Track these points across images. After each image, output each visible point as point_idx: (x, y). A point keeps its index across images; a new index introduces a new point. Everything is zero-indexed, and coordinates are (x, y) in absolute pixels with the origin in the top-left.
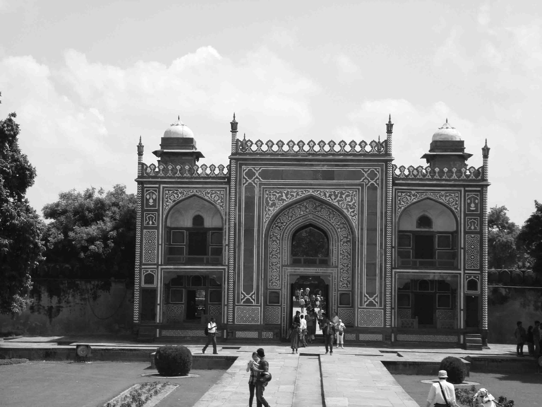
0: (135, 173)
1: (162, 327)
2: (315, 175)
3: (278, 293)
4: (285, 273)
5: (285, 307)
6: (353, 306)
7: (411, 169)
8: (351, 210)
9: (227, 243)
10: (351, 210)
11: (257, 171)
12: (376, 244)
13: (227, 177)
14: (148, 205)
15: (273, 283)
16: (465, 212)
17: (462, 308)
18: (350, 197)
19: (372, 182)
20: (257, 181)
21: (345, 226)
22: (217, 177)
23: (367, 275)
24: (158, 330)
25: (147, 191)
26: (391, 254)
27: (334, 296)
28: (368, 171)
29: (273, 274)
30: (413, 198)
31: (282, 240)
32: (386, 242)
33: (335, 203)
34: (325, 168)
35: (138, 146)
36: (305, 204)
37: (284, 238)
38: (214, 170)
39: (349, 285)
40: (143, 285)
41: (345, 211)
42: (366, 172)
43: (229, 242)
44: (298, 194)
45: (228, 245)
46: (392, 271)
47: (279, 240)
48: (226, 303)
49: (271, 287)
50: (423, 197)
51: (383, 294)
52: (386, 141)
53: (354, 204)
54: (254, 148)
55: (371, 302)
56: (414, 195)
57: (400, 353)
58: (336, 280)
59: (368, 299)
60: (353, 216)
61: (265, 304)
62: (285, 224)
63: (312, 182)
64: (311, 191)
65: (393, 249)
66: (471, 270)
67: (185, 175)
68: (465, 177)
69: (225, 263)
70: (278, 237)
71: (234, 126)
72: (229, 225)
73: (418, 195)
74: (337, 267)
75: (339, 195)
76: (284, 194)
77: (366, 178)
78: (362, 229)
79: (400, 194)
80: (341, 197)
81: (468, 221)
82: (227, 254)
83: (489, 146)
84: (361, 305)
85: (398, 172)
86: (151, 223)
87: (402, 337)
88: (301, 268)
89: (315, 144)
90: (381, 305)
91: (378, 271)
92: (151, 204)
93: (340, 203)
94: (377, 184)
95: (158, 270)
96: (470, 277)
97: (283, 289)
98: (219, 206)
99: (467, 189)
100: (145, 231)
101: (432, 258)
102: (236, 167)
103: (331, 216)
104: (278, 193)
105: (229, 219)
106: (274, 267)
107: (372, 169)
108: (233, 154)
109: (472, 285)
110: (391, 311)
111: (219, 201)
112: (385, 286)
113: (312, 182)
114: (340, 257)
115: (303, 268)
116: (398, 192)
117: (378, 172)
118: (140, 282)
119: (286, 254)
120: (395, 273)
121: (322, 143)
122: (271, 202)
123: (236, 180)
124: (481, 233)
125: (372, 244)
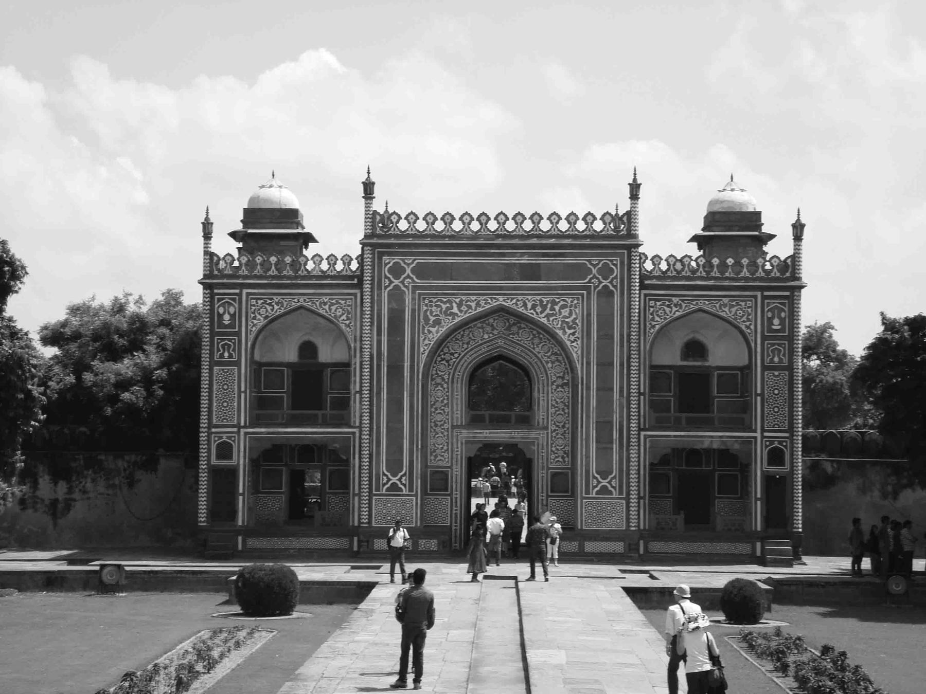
0: (198, 271)
1: (248, 532)
2: (508, 272)
3: (445, 474)
5: (458, 496)
6: (573, 494)
7: (672, 260)
8: (569, 332)
9: (358, 389)
11: (408, 265)
12: (612, 389)
13: (357, 276)
14: (221, 325)
15: (436, 456)
16: (762, 332)
17: (759, 496)
19: (605, 283)
20: (408, 281)
21: (560, 358)
22: (339, 276)
23: (597, 442)
24: (240, 538)
25: (219, 300)
26: (638, 406)
27: (541, 476)
28: (598, 264)
29: (438, 441)
30: (674, 309)
31: (452, 382)
32: (629, 385)
33: (542, 320)
34: (525, 260)
35: (203, 223)
36: (491, 321)
37: (455, 380)
38: (335, 263)
39: (566, 459)
40: (214, 461)
41: (560, 332)
42: (594, 266)
43: (361, 387)
44: (478, 305)
45: (360, 392)
46: (639, 434)
48: (357, 492)
49: (434, 463)
50: (693, 307)
51: (624, 473)
52: (629, 214)
53: (574, 321)
54: (403, 225)
55: (604, 487)
56: (676, 305)
57: (654, 574)
59: (599, 482)
60: (572, 342)
61: (424, 492)
62: (456, 355)
64: (501, 298)
65: (642, 397)
66: (774, 432)
67: (285, 273)
68: (763, 274)
69: (355, 422)
70: (446, 377)
71: (368, 188)
72: (361, 357)
73: (684, 305)
74: (546, 428)
75: (549, 306)
76: (454, 304)
77: (594, 277)
78: (588, 364)
79: (652, 303)
80: (552, 309)
81: (768, 348)
82: (359, 407)
83: (803, 221)
84: (587, 492)
85: (648, 266)
86: (226, 354)
87: (657, 546)
88: (485, 431)
89: (507, 219)
90: (621, 493)
91: (615, 435)
92: (227, 323)
93: (551, 319)
94: (614, 286)
95: (239, 436)
96: (772, 443)
97: (454, 466)
98: (343, 326)
99: (766, 293)
100: (216, 368)
101: (708, 413)
102: (373, 258)
103: (536, 341)
104: (445, 303)
105: (361, 348)
106: (438, 429)
107: (605, 260)
108: (366, 236)
109: (776, 456)
110: (639, 503)
111: (344, 317)
112: (628, 461)
114: (552, 410)
115: (488, 431)
116: (650, 300)
117: (616, 265)
118: (209, 457)
121: (519, 217)
122: (432, 319)
123: (373, 280)
124: (790, 368)
125: (605, 388)
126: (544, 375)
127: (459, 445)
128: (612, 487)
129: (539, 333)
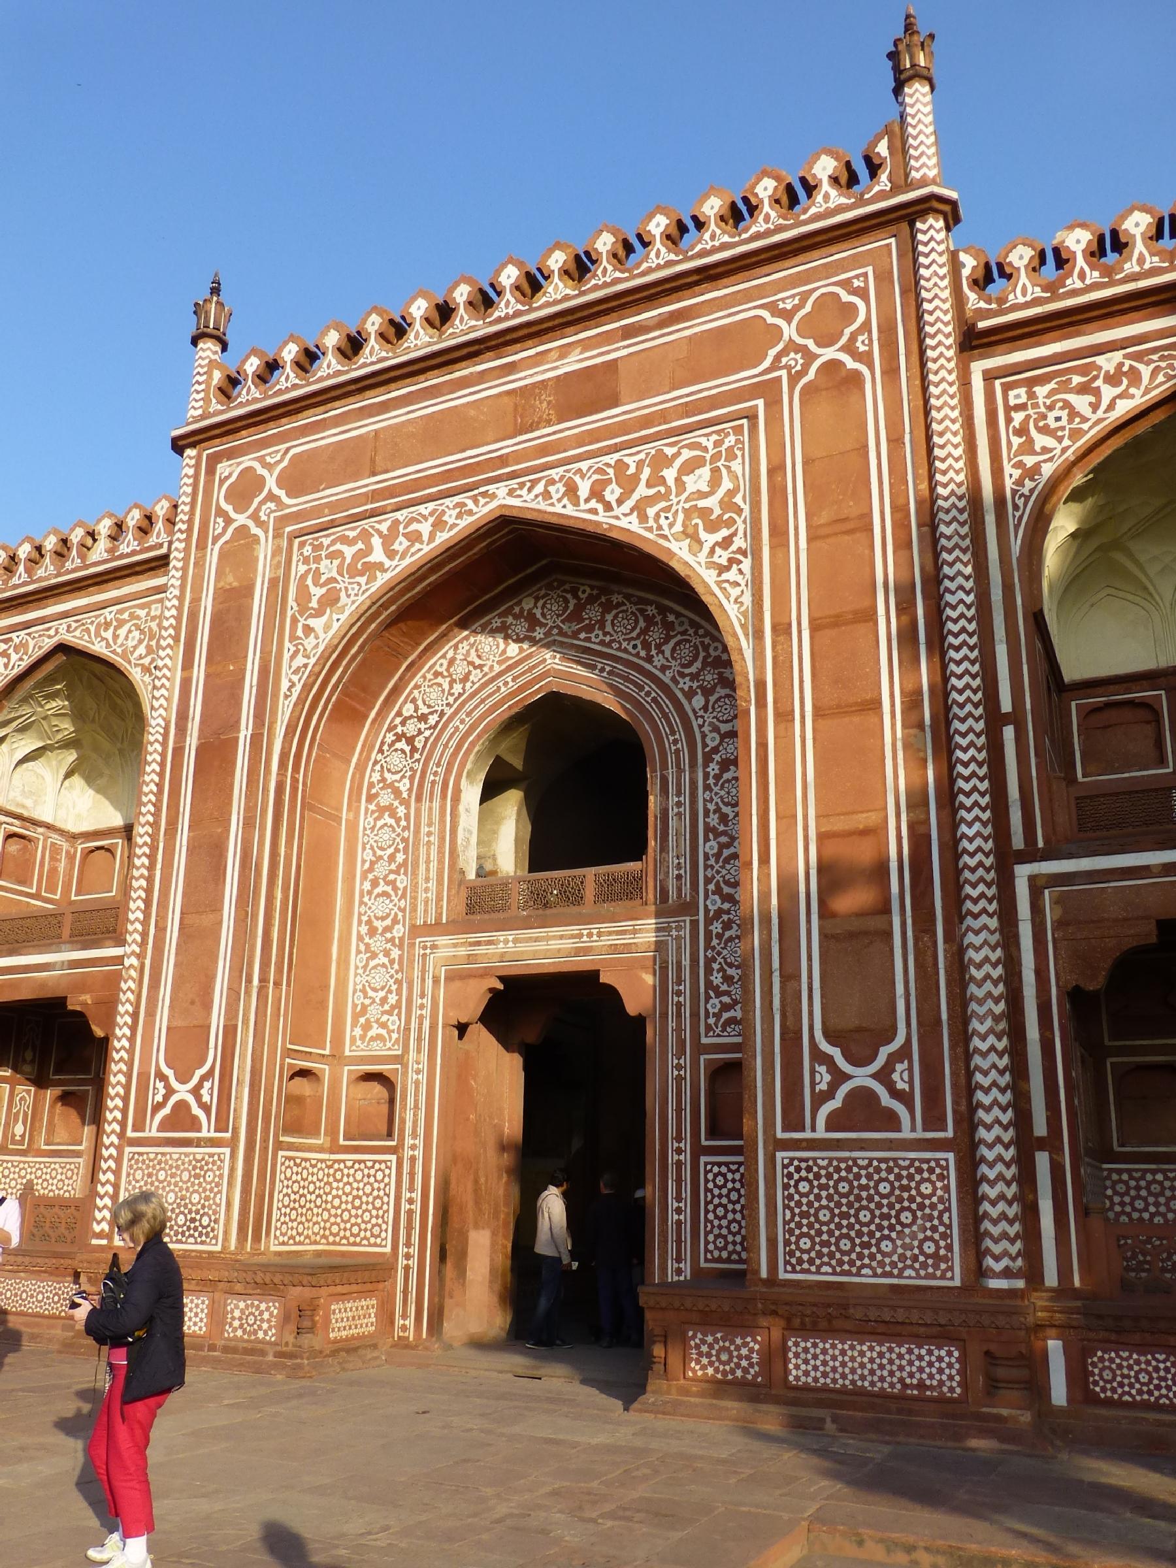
2: (521, 412)
4: (423, 971)
8: (709, 539)
10: (709, 539)
12: (875, 705)
15: (367, 1027)
18: (705, 472)
31: (419, 799)
33: (623, 523)
36: (527, 604)
37: (427, 786)
47: (406, 803)
55: (863, 1097)
58: (686, 987)
59: (840, 1077)
62: (432, 720)
63: (507, 446)
70: (404, 786)
74: (689, 908)
76: (376, 541)
78: (782, 629)
87: (1128, 1374)
88: (501, 936)
93: (651, 512)
103: (655, 635)
104: (350, 542)
106: (377, 943)
113: (507, 446)
115: (510, 935)
119: (434, 866)
120: (1036, 886)
122: (317, 592)
126: (681, 735)
127: (429, 982)
128: (895, 1094)
129: (663, 610)
